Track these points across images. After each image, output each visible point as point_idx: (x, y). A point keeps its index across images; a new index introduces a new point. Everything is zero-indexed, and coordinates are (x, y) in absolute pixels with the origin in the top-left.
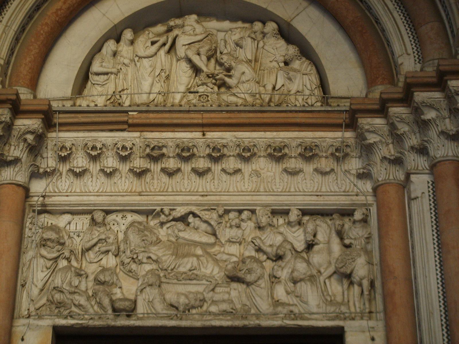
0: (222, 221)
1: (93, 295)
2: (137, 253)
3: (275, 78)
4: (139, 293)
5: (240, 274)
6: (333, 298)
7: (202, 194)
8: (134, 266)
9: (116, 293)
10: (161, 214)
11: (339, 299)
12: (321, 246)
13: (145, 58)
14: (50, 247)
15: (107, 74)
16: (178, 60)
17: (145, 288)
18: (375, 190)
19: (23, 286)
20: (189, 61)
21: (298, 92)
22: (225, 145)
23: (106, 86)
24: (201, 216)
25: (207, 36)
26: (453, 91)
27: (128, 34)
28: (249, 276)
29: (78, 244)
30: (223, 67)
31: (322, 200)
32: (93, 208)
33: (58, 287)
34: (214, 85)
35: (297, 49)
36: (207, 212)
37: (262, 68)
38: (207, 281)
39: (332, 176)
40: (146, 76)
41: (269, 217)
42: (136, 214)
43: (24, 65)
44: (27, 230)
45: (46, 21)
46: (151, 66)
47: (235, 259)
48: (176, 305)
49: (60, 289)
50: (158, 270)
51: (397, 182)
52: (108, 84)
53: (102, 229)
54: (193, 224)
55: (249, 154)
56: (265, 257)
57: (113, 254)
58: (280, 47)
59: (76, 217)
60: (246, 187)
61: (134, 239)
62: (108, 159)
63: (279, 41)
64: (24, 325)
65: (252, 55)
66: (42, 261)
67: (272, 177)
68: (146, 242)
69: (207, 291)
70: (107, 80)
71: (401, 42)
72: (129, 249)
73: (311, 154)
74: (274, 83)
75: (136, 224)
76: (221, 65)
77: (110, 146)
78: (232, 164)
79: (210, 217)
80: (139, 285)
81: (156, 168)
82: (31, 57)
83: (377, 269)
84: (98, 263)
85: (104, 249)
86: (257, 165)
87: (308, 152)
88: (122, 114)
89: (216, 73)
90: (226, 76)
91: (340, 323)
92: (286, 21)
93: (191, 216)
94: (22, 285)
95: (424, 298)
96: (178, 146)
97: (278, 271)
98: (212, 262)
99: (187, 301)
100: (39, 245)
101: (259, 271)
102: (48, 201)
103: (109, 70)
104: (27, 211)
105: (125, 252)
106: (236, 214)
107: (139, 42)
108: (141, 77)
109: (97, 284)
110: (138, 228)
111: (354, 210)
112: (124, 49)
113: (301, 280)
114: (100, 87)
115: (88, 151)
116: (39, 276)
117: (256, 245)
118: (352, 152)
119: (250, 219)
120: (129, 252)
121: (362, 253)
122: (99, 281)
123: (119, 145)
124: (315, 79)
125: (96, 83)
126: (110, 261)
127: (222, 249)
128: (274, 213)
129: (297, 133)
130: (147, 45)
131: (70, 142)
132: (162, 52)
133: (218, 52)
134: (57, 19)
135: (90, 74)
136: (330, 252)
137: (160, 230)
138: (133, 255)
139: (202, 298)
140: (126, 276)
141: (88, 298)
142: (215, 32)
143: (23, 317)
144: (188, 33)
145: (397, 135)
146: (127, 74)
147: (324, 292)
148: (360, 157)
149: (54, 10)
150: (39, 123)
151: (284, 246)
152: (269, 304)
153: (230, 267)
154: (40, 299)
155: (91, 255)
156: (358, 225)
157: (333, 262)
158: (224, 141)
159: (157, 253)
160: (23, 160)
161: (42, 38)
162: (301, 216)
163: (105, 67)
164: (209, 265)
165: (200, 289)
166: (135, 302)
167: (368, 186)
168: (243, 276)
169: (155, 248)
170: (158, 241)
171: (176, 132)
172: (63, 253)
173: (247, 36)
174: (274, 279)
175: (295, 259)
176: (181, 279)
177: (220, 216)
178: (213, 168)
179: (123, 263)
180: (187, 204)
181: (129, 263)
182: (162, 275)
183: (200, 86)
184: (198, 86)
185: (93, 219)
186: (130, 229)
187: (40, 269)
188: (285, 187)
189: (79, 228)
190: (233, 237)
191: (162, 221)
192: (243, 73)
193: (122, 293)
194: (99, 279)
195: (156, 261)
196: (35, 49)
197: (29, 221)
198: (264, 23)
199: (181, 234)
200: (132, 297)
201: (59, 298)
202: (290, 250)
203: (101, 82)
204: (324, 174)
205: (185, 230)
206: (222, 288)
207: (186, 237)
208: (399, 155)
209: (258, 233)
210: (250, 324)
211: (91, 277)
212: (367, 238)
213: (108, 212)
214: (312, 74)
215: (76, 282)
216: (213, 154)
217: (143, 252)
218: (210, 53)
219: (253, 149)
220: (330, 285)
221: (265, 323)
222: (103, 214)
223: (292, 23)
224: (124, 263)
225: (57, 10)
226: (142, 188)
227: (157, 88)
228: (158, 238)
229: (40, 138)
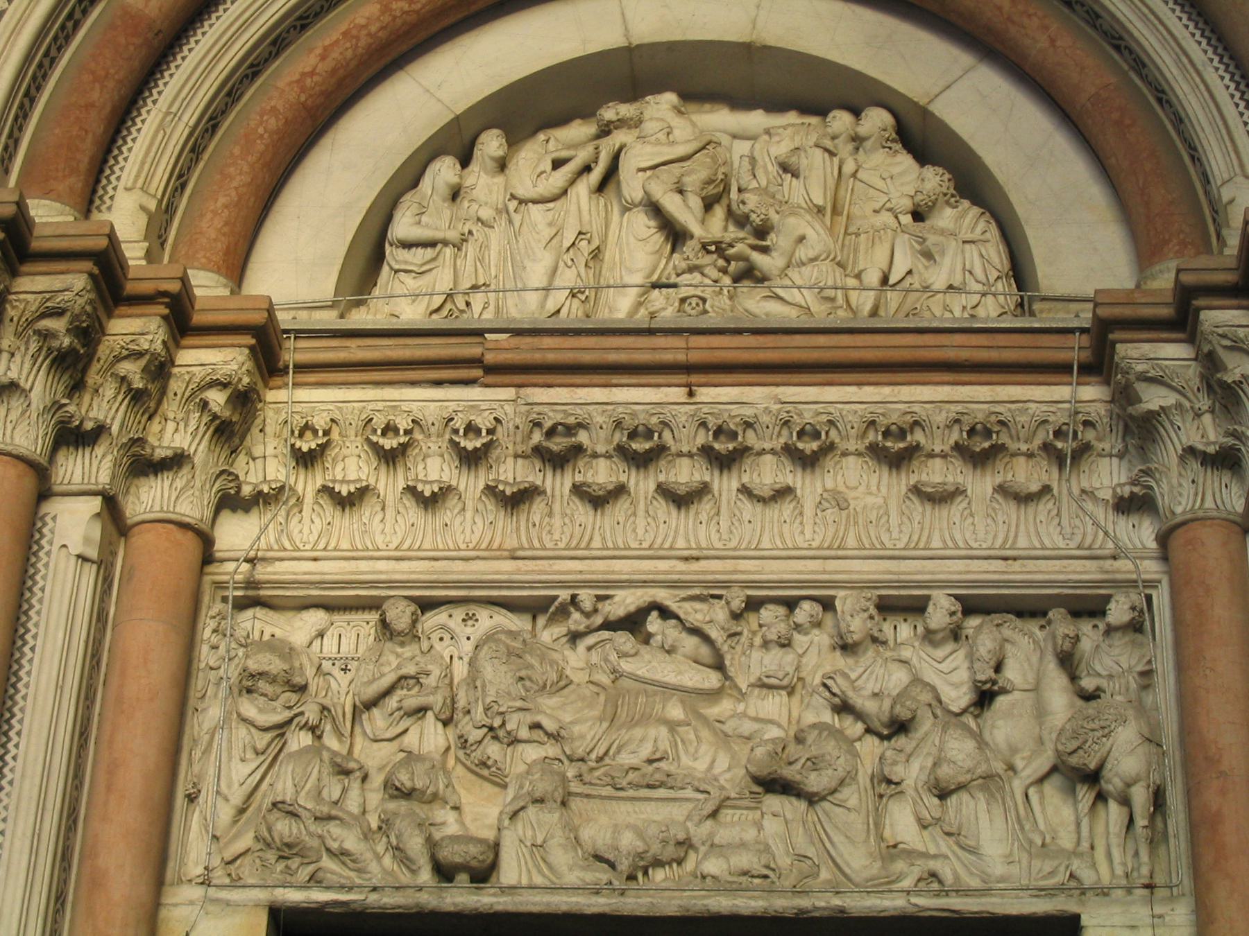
0: (739, 629)
1: (380, 828)
2: (502, 713)
3: (887, 253)
4: (507, 822)
5: (790, 773)
6: (1048, 840)
7: (686, 553)
8: (493, 750)
9: (443, 824)
10: (572, 609)
11: (1066, 841)
12: (1017, 695)
13: (535, 202)
14: (265, 695)
15: (432, 244)
16: (625, 209)
17: (523, 808)
18: (1164, 539)
19: (191, 798)
20: (655, 209)
21: (951, 287)
22: (751, 420)
24: (682, 616)
25: (704, 148)
27: (491, 144)
28: (813, 776)
29: (343, 693)
30: (748, 227)
31: (1019, 570)
32: (383, 593)
33: (283, 802)
34: (721, 274)
35: (947, 176)
36: (698, 605)
37: (852, 229)
38: (698, 790)
39: (1044, 508)
41: (871, 617)
42: (504, 611)
43: (209, 215)
44: (205, 648)
45: (273, 103)
46: (550, 224)
47: (774, 732)
48: (611, 857)
49: (291, 808)
50: (560, 760)
51: (1224, 515)
52: (434, 271)
53: (408, 651)
54: (659, 638)
55: (815, 445)
56: (859, 727)
57: (437, 719)
58: (901, 174)
59: (340, 619)
60: (808, 535)
61: (496, 676)
62: (429, 461)
64: (192, 903)
65: (825, 194)
66: (242, 732)
67: (880, 507)
68: (528, 683)
69: (696, 818)
70: (434, 259)
72: (480, 702)
73: (986, 445)
74: (885, 266)
75: (503, 637)
76: (741, 221)
77: (433, 424)
79: (707, 619)
80: (509, 799)
81: (558, 484)
82: (229, 195)
84: (395, 744)
85: (412, 702)
86: (839, 477)
87: (977, 439)
88: (468, 340)
89: (728, 240)
91: (1071, 907)
92: (916, 104)
93: (655, 614)
94: (188, 796)
96: (618, 424)
97: (895, 763)
99: (640, 846)
100: (236, 690)
101: (842, 760)
102: (264, 572)
103: (439, 235)
104: (206, 599)
105: (469, 712)
106: (781, 611)
107: (521, 163)
108: (523, 251)
109: (392, 797)
110: (507, 647)
111: (1108, 598)
112: (479, 179)
113: (961, 787)
114: (415, 278)
115: (374, 439)
116: (234, 773)
117: (834, 695)
118: (1100, 440)
119: (818, 624)
120: (480, 709)
121: (1130, 713)
122: (397, 789)
123: (459, 423)
124: (996, 254)
127: (741, 708)
128: (887, 607)
129: (947, 389)
131: (325, 414)
132: (583, 189)
133: (734, 189)
134: (303, 98)
135: (387, 245)
136: (1040, 712)
137: (568, 653)
138: (492, 718)
139: (681, 836)
140: (473, 777)
141: (367, 835)
142: (725, 140)
143: (190, 881)
145: (1225, 386)
147: (1021, 822)
148: (1121, 456)
149: (297, 77)
150: (241, 359)
151: (913, 694)
152: (871, 854)
153: (760, 752)
154: (237, 836)
155: (378, 720)
156: (1119, 640)
158: (748, 412)
160: (198, 460)
161: (260, 146)
162: (959, 615)
164: (704, 748)
166: (496, 847)
167: (1143, 533)
168: (798, 778)
169: (554, 701)
170: (562, 684)
171: (616, 386)
172: (302, 713)
173: (811, 143)
174: (886, 784)
175: (944, 730)
176: (624, 784)
177: (736, 616)
178: (715, 487)
179: (464, 743)
180: (645, 583)
181: (480, 742)
182: (570, 774)
183: (683, 273)
185: (384, 623)
186: (486, 648)
187: (236, 754)
188: (915, 538)
189: (347, 647)
190: (771, 673)
191: (573, 628)
192: (802, 239)
193: (461, 822)
194: (397, 784)
195: (555, 737)
196: (240, 174)
197: (212, 624)
198: (856, 113)
199: (626, 666)
200: (490, 835)
201: (286, 832)
202: (930, 705)
203: (415, 265)
204: (1024, 499)
205: (636, 654)
206: (738, 812)
207: (639, 673)
208: (1231, 441)
209: (840, 661)
210: (816, 908)
211: (377, 780)
213: (426, 605)
214: (988, 241)
215: (333, 790)
216: (717, 446)
217: (521, 709)
218: (711, 190)
219: (827, 433)
220: (1042, 803)
222: (413, 607)
223: (932, 108)
224: (466, 741)
225: (304, 75)
226: (519, 538)
227: (568, 277)
228: (561, 675)
229: (245, 400)
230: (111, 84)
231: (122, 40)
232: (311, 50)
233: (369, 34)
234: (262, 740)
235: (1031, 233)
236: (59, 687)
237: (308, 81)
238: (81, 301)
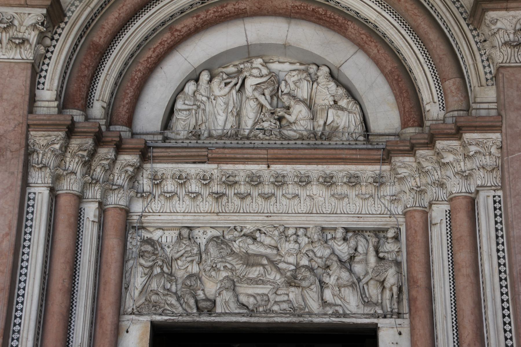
3: (326, 115)
4: (218, 295)
7: (267, 215)
8: (213, 273)
9: (199, 295)
19: (126, 289)
23: (188, 121)
26: (467, 142)
35: (345, 90)
37: (316, 105)
40: (221, 112)
43: (122, 107)
44: (128, 243)
45: (139, 68)
48: (246, 304)
63: (330, 83)
66: (140, 269)
71: (429, 91)
75: (215, 239)
78: (292, 189)
80: (218, 288)
81: (230, 192)
83: (404, 279)
90: (285, 113)
91: (375, 321)
95: (440, 304)
98: (275, 270)
103: (191, 107)
120: (209, 261)
121: (393, 265)
124: (359, 118)
125: (180, 117)
126: (195, 269)
129: (343, 166)
130: (221, 86)
133: (280, 91)
135: (175, 109)
144: (255, 75)
146: (205, 110)
149: (146, 59)
150: (137, 158)
157: (370, 271)
158: (285, 172)
159: (231, 262)
163: (187, 105)
164: (273, 273)
165: (265, 291)
166: (214, 302)
172: (157, 262)
182: (235, 280)
184: (263, 122)
185: (180, 234)
187: (139, 275)
188: (333, 210)
192: (301, 111)
193: (205, 294)
211: (180, 281)
212: (397, 252)
218: (274, 93)
220: (368, 289)
221: (316, 320)
225: (148, 58)
228: (232, 250)
230: (91, 68)
231: (93, 53)
232: (150, 49)
233: (168, 43)
234: (146, 271)
235: (369, 111)
236: (90, 261)
237: (150, 60)
238: (91, 147)
